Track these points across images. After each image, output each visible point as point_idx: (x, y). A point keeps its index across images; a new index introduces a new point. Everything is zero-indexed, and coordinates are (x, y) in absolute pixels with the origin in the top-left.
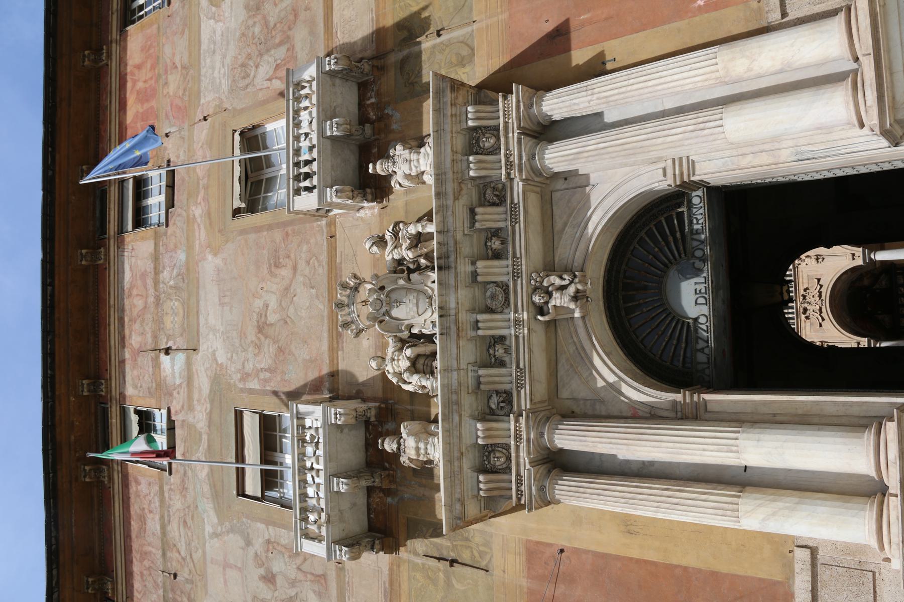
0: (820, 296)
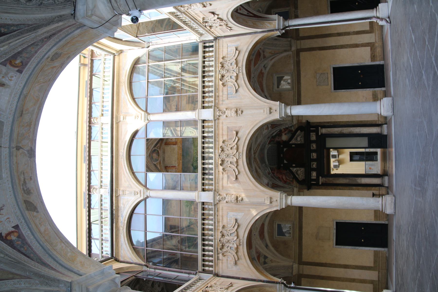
0: (237, 149)
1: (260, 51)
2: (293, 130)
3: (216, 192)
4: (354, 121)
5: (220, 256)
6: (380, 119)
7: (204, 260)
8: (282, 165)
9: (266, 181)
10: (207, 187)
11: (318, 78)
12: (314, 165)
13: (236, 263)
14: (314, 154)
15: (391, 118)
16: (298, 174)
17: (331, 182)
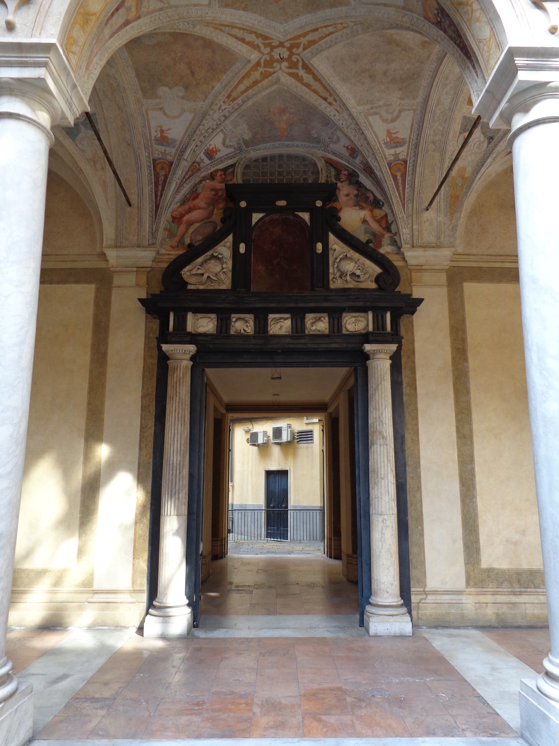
4: (419, 489)
6: (430, 598)
12: (243, 325)
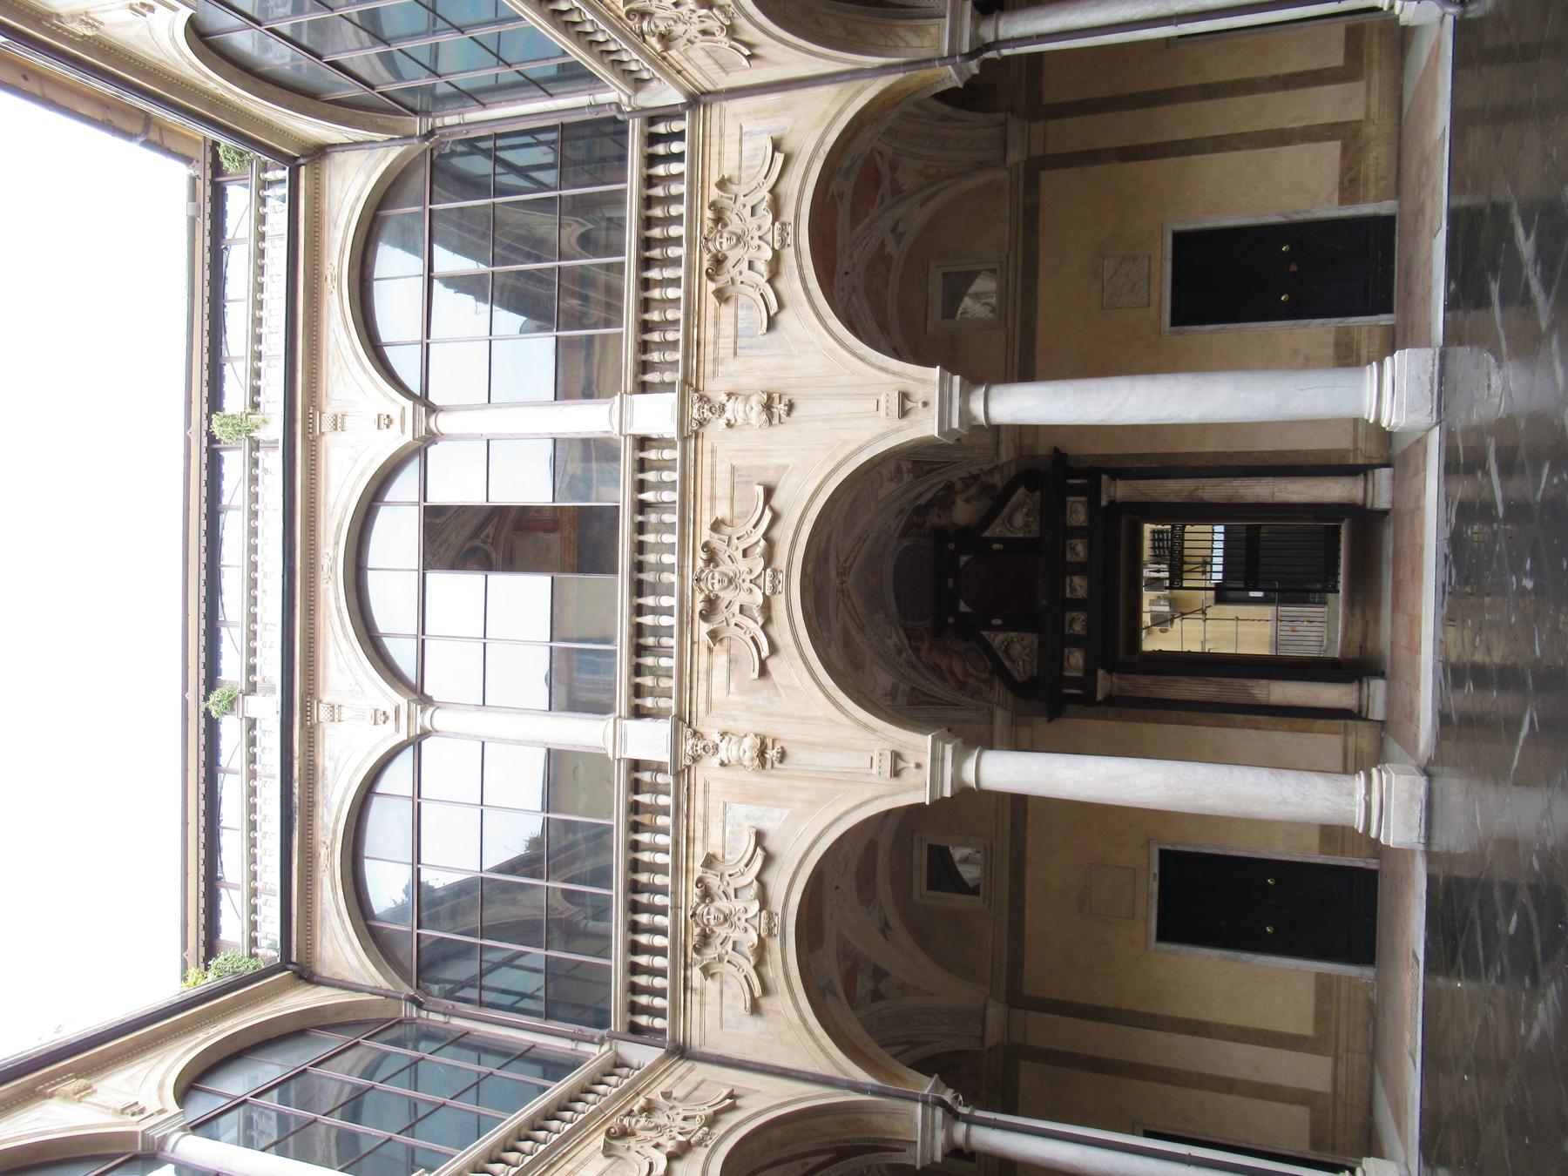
0: (769, 556)
1: (879, 162)
2: (1000, 485)
3: (682, 721)
4: (1249, 453)
5: (696, 974)
6: (1361, 445)
7: (634, 989)
8: (951, 620)
9: (885, 680)
10: (649, 702)
11: (1106, 276)
12: (1077, 624)
13: (755, 1008)
14: (1076, 579)
15: (1421, 442)
16: (1009, 657)
17: (1144, 694)
